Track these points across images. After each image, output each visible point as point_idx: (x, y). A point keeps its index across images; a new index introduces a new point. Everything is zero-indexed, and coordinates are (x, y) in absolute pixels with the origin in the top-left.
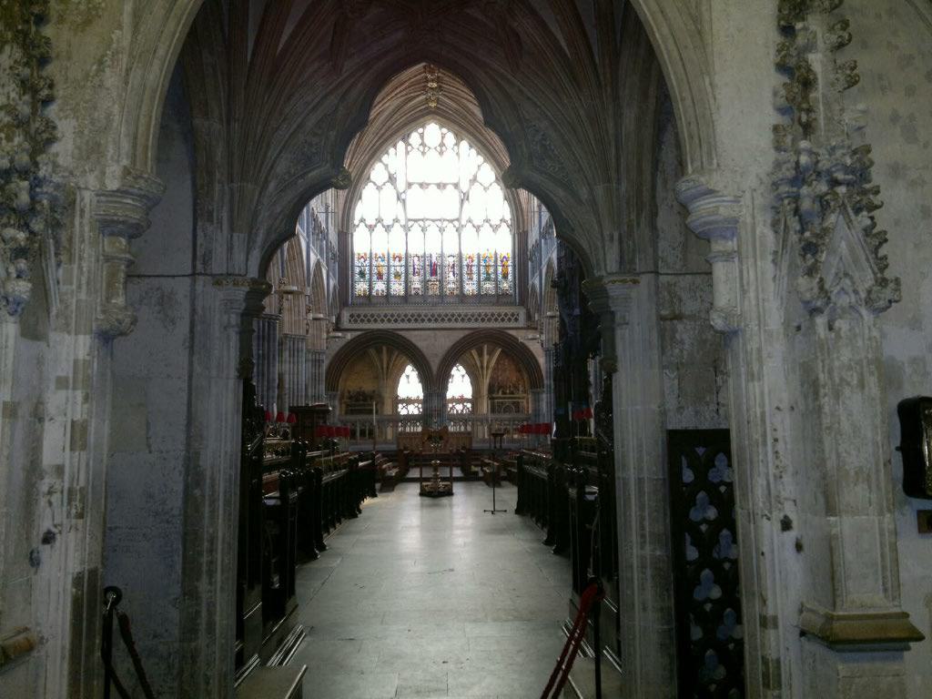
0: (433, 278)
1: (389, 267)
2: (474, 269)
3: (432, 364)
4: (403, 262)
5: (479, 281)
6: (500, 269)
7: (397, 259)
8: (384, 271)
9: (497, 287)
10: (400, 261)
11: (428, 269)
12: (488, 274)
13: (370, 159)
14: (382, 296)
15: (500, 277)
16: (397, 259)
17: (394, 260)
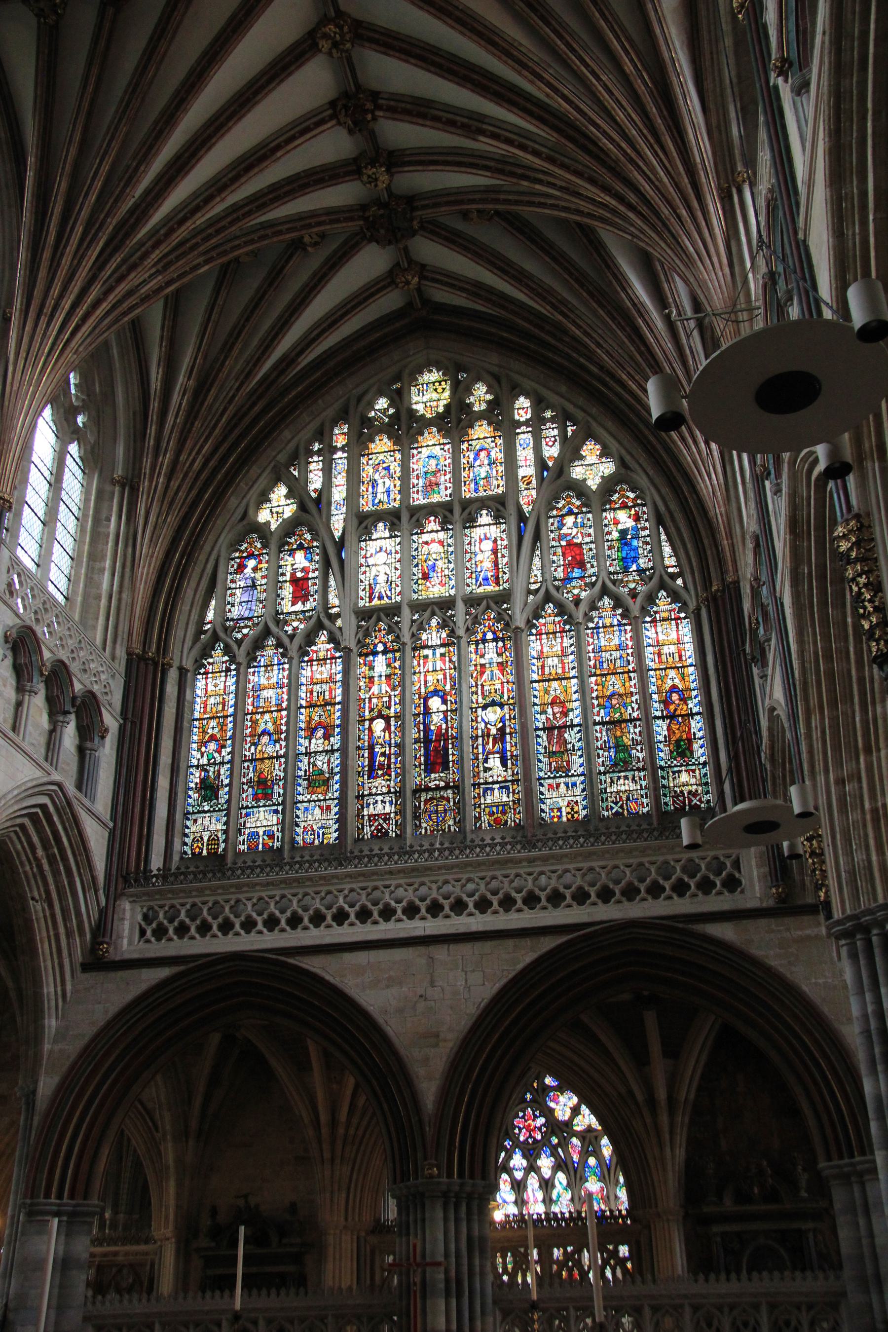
0: (435, 779)
1: (291, 758)
2: (572, 736)
3: (419, 1071)
4: (336, 741)
5: (590, 776)
6: (661, 728)
7: (320, 733)
8: (278, 770)
9: (656, 789)
10: (326, 737)
11: (416, 752)
12: (619, 747)
13: (245, 460)
14: (268, 849)
15: (663, 755)
16: (320, 733)
17: (310, 737)
